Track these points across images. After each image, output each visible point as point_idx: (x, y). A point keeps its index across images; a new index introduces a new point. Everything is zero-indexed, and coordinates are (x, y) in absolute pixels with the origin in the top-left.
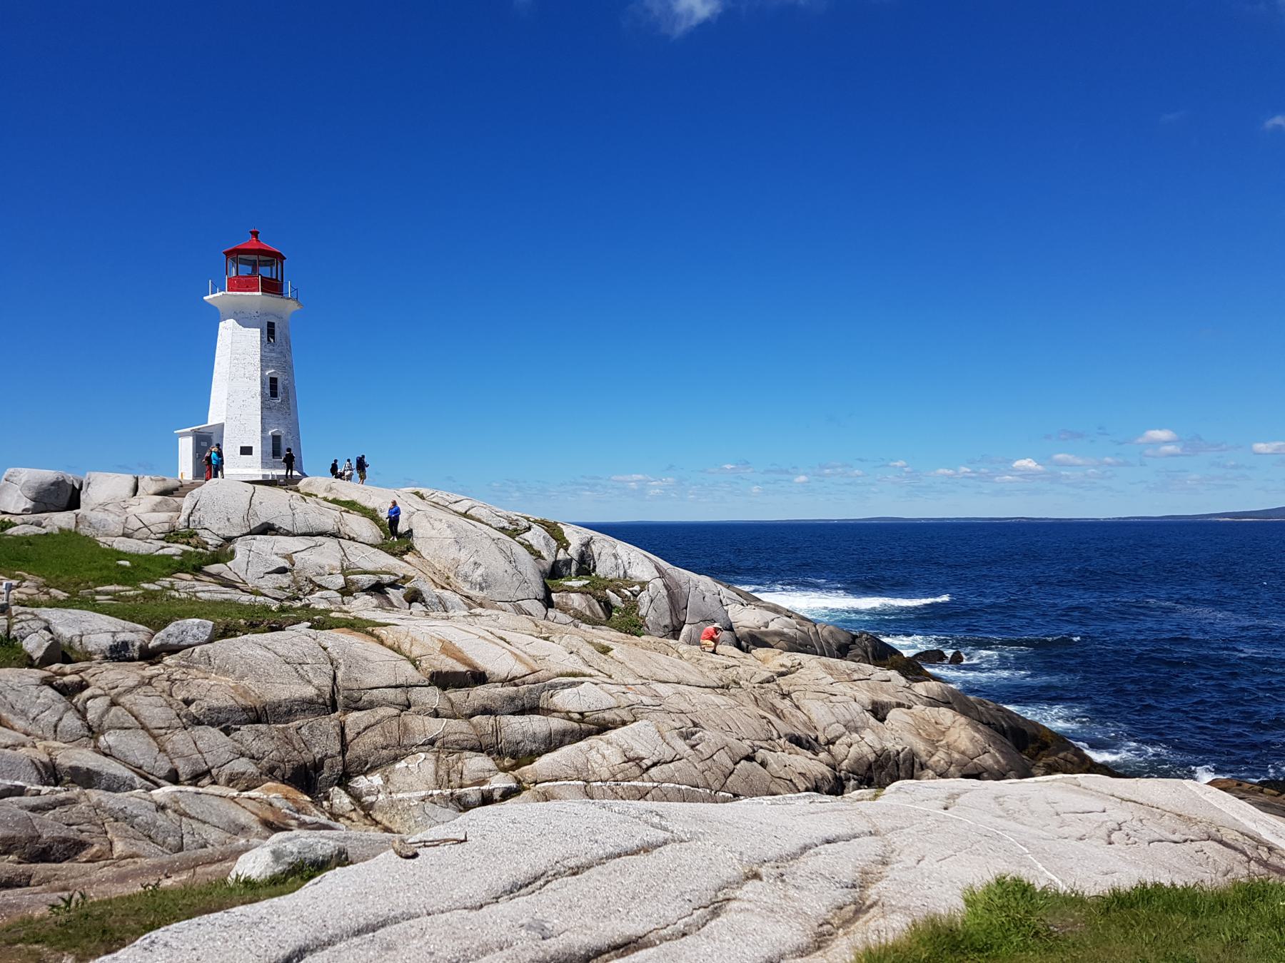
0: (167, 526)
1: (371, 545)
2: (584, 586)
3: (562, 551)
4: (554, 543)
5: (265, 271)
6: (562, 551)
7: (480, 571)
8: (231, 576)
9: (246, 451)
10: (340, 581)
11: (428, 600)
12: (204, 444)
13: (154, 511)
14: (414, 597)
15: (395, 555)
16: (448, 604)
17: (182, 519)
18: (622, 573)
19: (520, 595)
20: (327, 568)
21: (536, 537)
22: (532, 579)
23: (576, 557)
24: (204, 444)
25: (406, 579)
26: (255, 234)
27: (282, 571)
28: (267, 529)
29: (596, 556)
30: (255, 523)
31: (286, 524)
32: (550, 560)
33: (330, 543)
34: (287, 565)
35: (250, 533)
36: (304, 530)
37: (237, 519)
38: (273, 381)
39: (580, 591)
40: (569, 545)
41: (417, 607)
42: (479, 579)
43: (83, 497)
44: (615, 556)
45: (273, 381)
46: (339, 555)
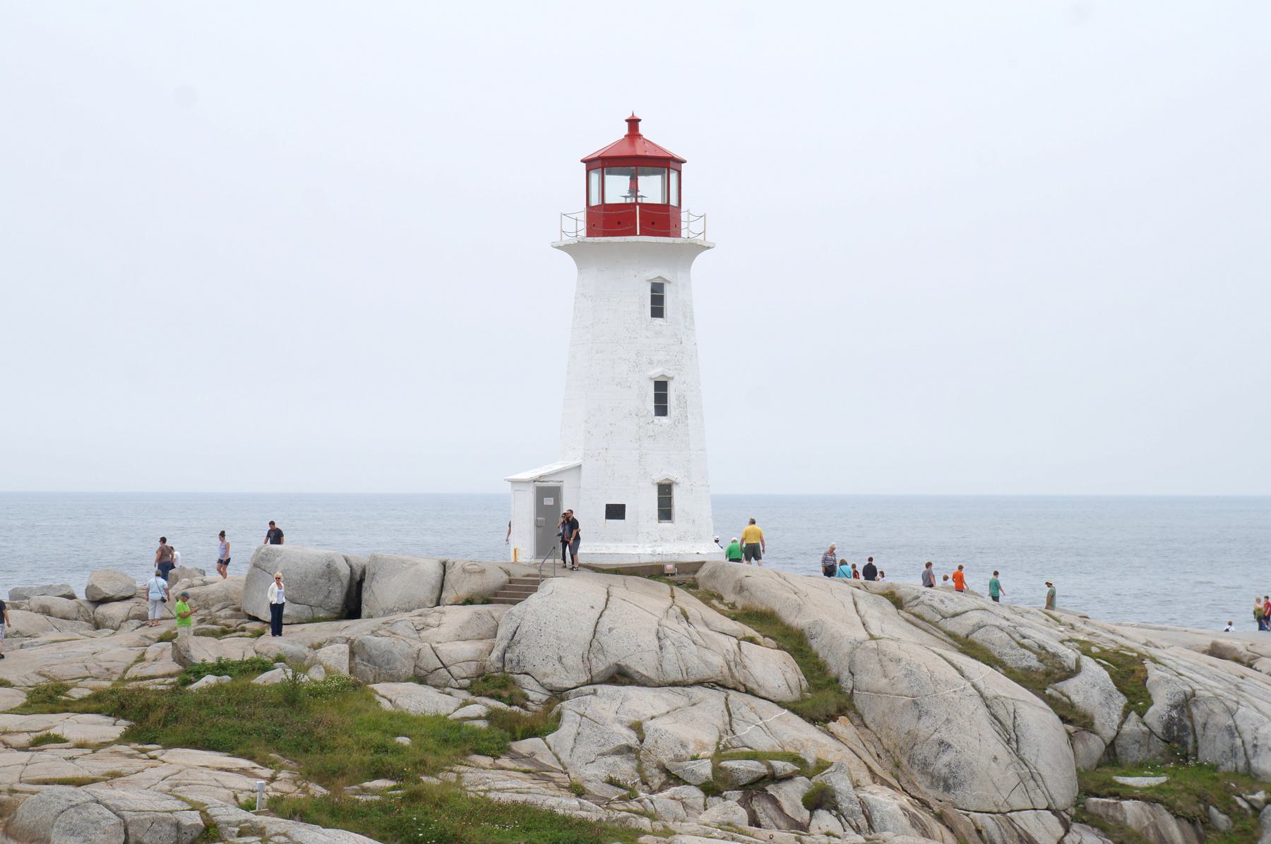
0: (473, 665)
1: (781, 704)
2: (1159, 788)
3: (1133, 716)
4: (1121, 701)
5: (651, 189)
6: (1133, 716)
7: (945, 758)
8: (547, 759)
9: (615, 512)
10: (705, 769)
11: (844, 805)
12: (549, 501)
13: (460, 638)
14: (820, 800)
15: (813, 720)
16: (876, 816)
17: (496, 654)
18: (1241, 764)
19: (1018, 800)
20: (692, 747)
21: (1091, 687)
22: (1045, 771)
23: (1158, 729)
24: (549, 501)
25: (822, 766)
26: (633, 123)
27: (625, 751)
28: (620, 676)
29: (1199, 729)
30: (600, 666)
31: (643, 664)
32: (1109, 733)
33: (714, 699)
34: (632, 739)
35: (591, 682)
36: (675, 676)
37: (572, 660)
38: (661, 388)
39: (1149, 797)
40: (1149, 703)
41: (825, 820)
42: (945, 771)
43: (365, 596)
44: (1233, 731)
45: (661, 388)
46: (720, 720)
